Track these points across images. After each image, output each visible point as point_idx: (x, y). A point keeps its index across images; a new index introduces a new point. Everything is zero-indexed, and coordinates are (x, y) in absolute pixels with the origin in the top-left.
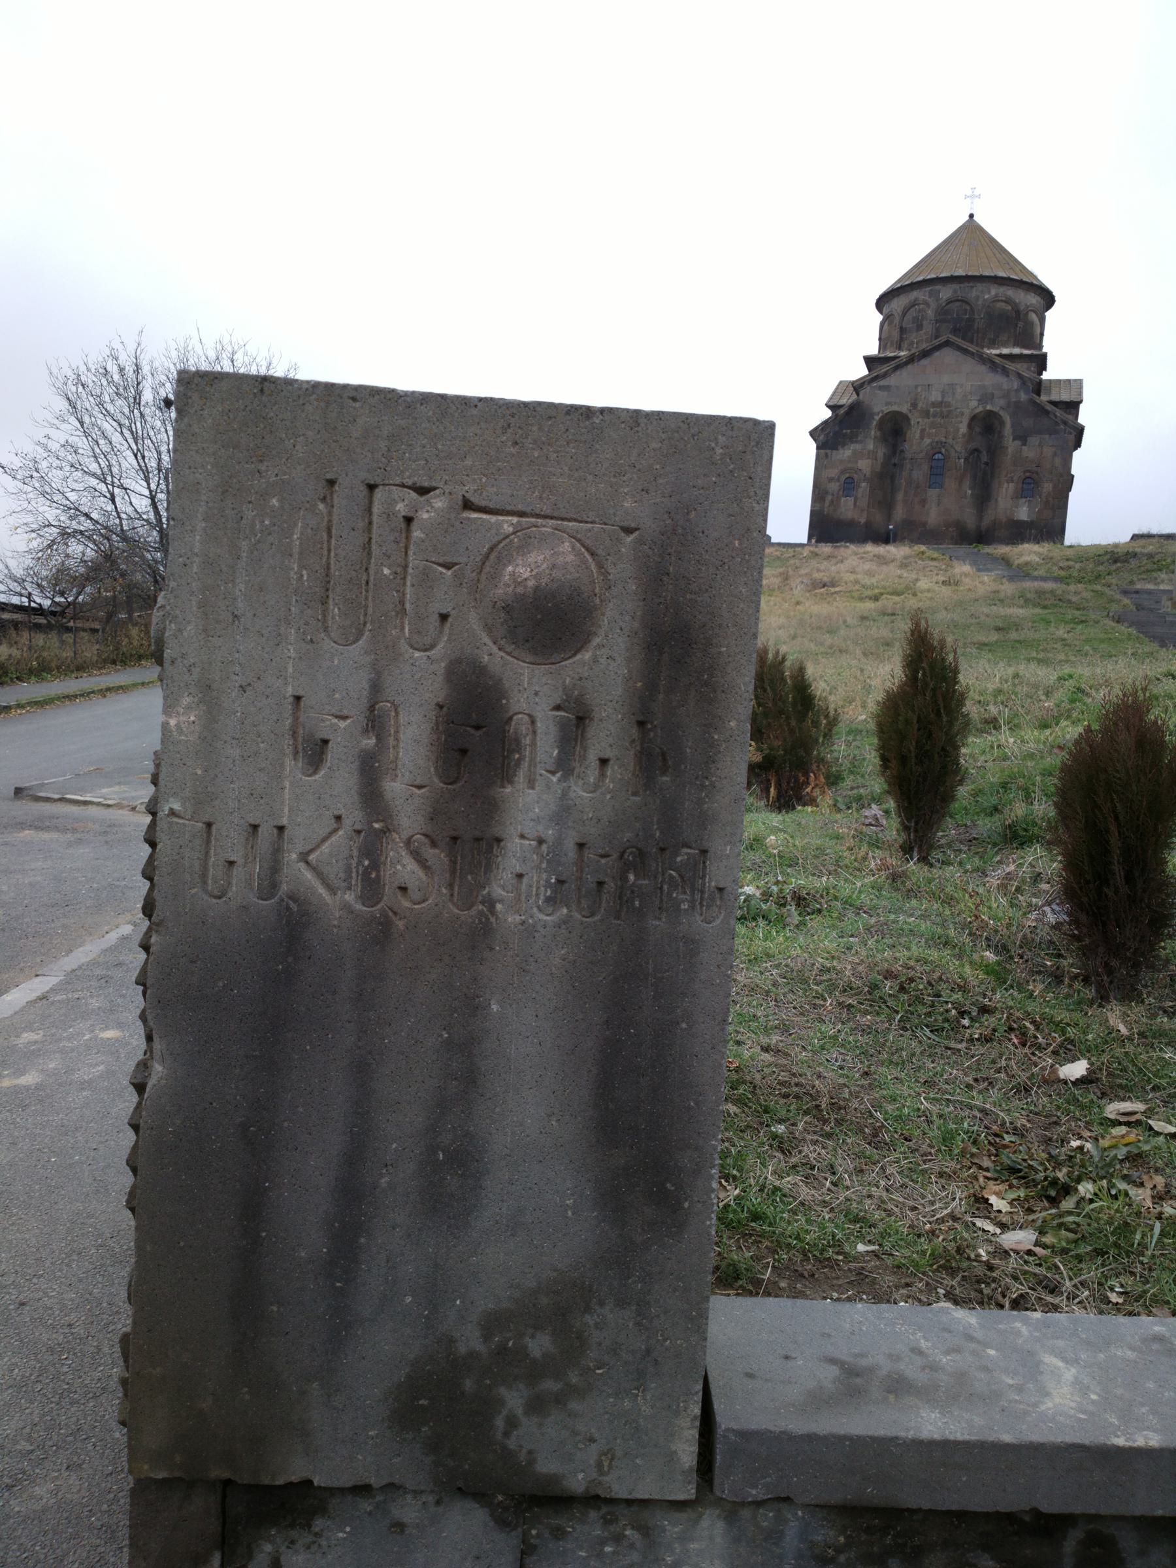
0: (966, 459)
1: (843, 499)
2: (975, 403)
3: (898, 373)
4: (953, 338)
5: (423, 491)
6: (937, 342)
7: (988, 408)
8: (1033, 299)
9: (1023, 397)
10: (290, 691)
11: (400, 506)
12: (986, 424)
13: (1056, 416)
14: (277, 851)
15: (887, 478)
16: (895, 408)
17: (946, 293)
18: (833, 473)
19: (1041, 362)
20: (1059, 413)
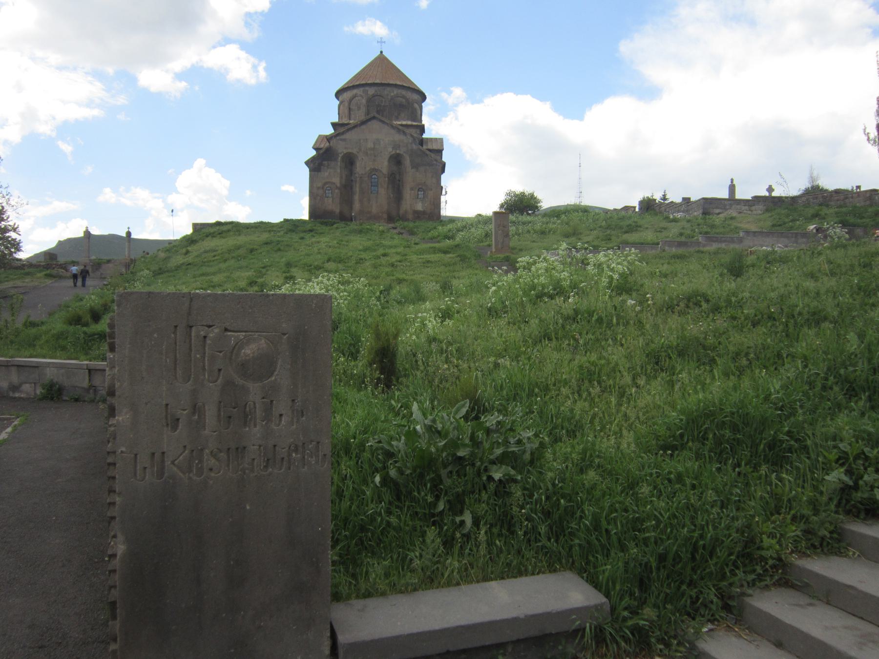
5: (210, 326)
6: (369, 117)
8: (416, 97)
9: (415, 147)
10: (164, 403)
11: (202, 333)
12: (396, 160)
14: (163, 461)
15: (347, 188)
16: (350, 151)
17: (371, 91)
18: (320, 185)
19: (422, 129)
20: (433, 155)
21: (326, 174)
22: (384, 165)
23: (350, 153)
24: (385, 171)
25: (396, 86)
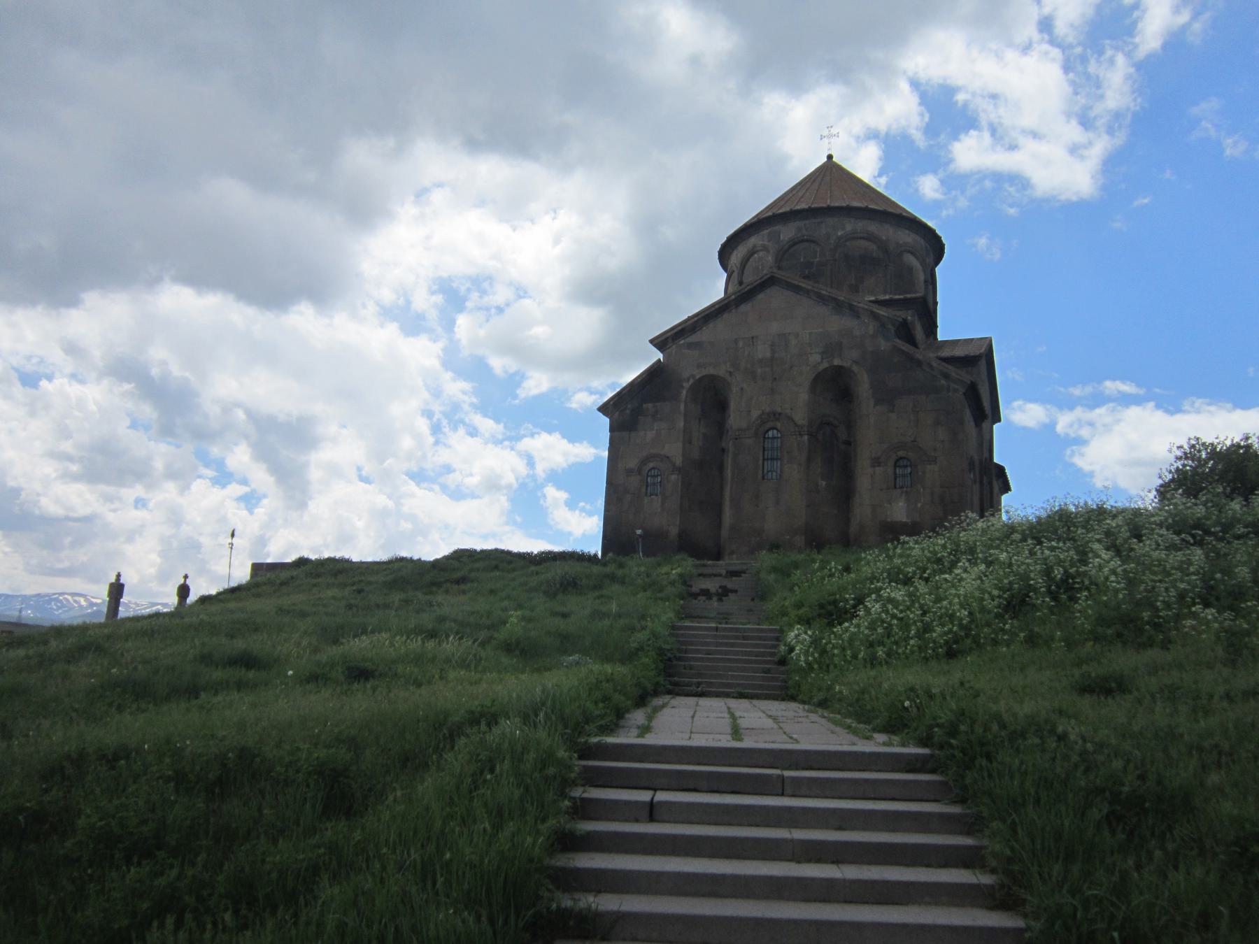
0: (810, 434)
1: (646, 500)
2: (817, 358)
3: (711, 325)
4: (779, 274)
7: (836, 362)
8: (907, 237)
9: (884, 345)
12: (835, 385)
13: (931, 367)
16: (711, 371)
17: (787, 232)
18: (633, 463)
21: (650, 435)
22: (798, 400)
23: (712, 378)
24: (800, 417)
25: (848, 211)
